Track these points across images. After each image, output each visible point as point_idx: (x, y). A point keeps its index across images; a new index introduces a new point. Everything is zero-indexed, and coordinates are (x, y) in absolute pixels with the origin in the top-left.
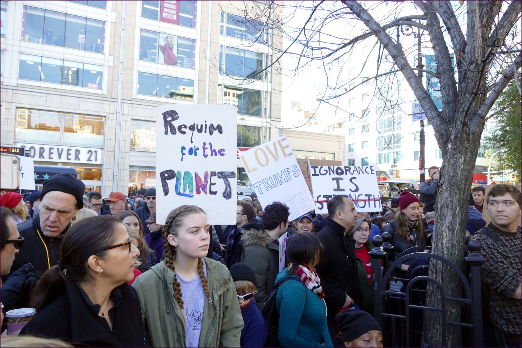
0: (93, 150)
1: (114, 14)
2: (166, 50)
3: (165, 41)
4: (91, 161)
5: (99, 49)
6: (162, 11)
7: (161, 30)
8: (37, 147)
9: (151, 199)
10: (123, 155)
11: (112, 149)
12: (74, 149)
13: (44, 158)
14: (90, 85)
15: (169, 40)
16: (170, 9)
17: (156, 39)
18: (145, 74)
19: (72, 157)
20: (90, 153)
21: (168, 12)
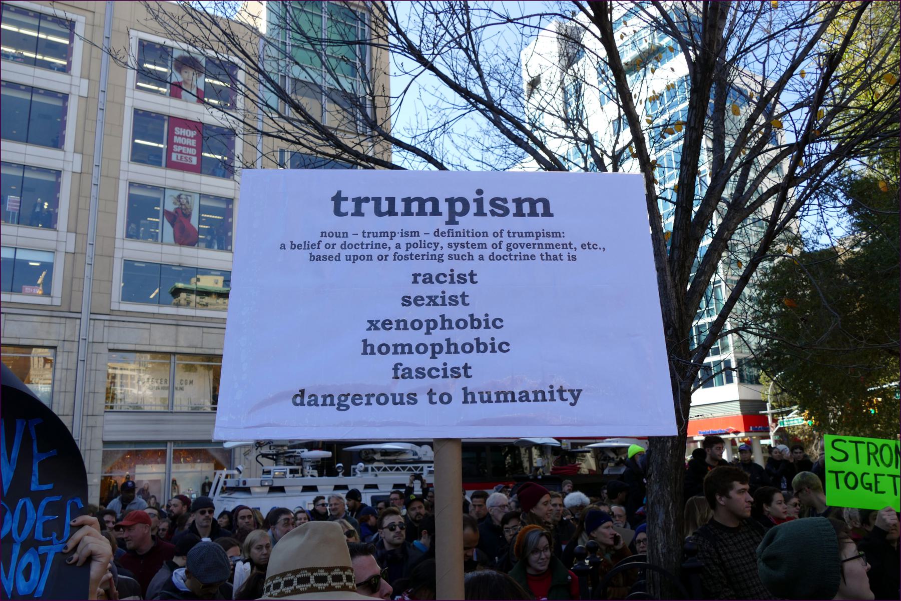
1: (78, 157)
2: (179, 218)
3: (175, 203)
5: (48, 221)
6: (170, 150)
7: (169, 183)
9: (207, 514)
10: (91, 421)
14: (27, 289)
15: (184, 201)
16: (185, 146)
17: (159, 200)
18: (136, 264)
21: (181, 152)
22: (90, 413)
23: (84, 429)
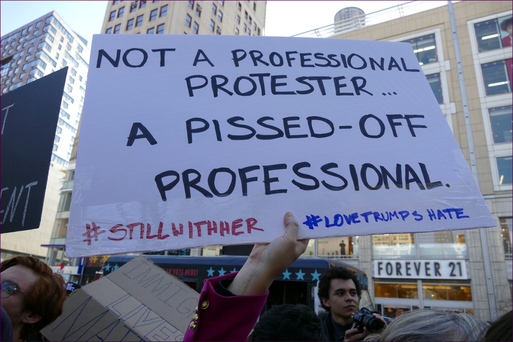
0: (455, 262)
4: (454, 275)
8: (393, 263)
11: (479, 259)
12: (432, 262)
13: (401, 274)
19: (432, 272)
20: (452, 266)
22: (495, 260)
23: (493, 271)
